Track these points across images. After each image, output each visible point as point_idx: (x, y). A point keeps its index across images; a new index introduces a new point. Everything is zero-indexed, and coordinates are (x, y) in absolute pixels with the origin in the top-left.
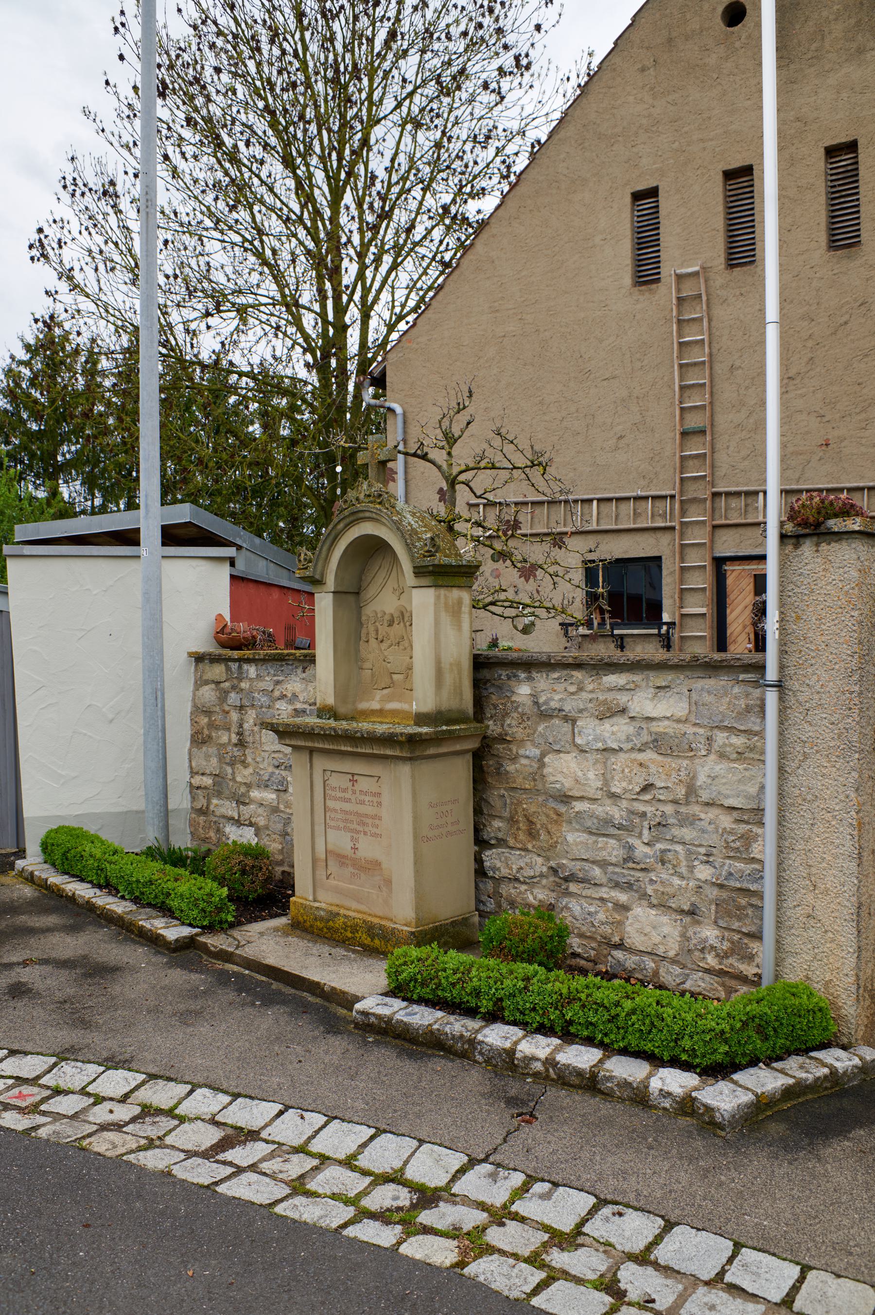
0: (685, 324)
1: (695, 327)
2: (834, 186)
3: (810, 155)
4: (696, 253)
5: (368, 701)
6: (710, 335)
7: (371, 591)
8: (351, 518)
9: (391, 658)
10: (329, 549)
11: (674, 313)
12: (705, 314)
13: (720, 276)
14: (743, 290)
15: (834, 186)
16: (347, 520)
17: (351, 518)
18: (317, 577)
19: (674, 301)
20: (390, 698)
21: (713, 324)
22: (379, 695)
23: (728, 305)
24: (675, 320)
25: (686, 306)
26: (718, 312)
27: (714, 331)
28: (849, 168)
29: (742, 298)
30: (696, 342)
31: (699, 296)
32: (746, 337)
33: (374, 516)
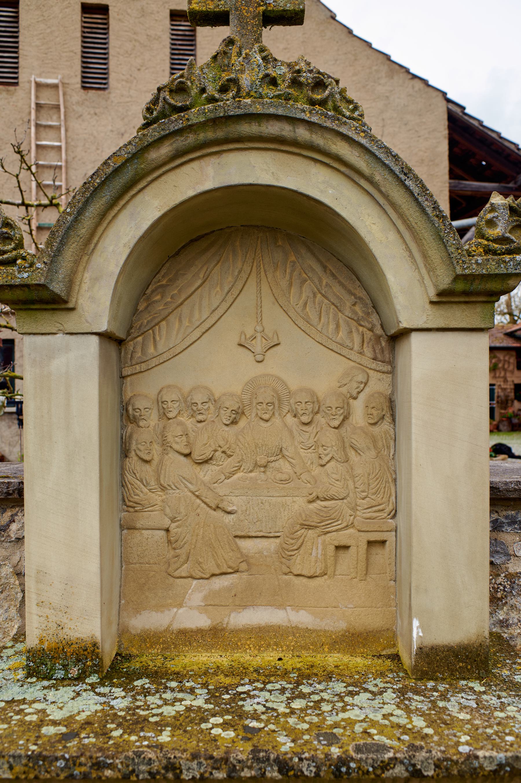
0: (42, 129)
1: (51, 133)
2: (175, 44)
3: (158, 12)
4: (54, 68)
5: (160, 607)
6: (66, 143)
7: (168, 337)
8: (210, 135)
9: (235, 502)
10: (103, 216)
11: (33, 116)
12: (63, 123)
13: (77, 94)
14: (97, 111)
15: (175, 44)
16: (180, 142)
17: (210, 135)
18: (57, 287)
19: (33, 106)
20: (245, 600)
21: (69, 134)
22: (196, 593)
23: (83, 121)
24: (33, 123)
25: (43, 112)
26: (74, 124)
27: (70, 140)
28: (187, 33)
29: (96, 117)
30: (53, 147)
31: (58, 107)
32: (99, 152)
33: (302, 133)
